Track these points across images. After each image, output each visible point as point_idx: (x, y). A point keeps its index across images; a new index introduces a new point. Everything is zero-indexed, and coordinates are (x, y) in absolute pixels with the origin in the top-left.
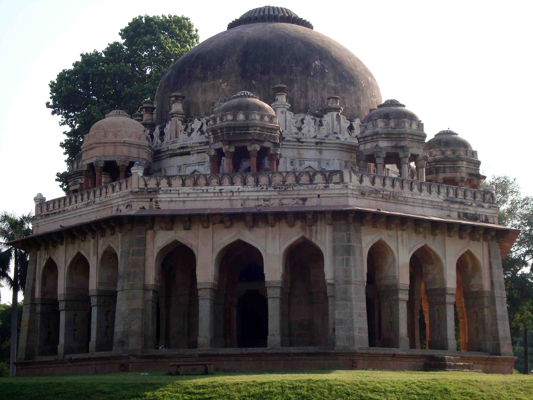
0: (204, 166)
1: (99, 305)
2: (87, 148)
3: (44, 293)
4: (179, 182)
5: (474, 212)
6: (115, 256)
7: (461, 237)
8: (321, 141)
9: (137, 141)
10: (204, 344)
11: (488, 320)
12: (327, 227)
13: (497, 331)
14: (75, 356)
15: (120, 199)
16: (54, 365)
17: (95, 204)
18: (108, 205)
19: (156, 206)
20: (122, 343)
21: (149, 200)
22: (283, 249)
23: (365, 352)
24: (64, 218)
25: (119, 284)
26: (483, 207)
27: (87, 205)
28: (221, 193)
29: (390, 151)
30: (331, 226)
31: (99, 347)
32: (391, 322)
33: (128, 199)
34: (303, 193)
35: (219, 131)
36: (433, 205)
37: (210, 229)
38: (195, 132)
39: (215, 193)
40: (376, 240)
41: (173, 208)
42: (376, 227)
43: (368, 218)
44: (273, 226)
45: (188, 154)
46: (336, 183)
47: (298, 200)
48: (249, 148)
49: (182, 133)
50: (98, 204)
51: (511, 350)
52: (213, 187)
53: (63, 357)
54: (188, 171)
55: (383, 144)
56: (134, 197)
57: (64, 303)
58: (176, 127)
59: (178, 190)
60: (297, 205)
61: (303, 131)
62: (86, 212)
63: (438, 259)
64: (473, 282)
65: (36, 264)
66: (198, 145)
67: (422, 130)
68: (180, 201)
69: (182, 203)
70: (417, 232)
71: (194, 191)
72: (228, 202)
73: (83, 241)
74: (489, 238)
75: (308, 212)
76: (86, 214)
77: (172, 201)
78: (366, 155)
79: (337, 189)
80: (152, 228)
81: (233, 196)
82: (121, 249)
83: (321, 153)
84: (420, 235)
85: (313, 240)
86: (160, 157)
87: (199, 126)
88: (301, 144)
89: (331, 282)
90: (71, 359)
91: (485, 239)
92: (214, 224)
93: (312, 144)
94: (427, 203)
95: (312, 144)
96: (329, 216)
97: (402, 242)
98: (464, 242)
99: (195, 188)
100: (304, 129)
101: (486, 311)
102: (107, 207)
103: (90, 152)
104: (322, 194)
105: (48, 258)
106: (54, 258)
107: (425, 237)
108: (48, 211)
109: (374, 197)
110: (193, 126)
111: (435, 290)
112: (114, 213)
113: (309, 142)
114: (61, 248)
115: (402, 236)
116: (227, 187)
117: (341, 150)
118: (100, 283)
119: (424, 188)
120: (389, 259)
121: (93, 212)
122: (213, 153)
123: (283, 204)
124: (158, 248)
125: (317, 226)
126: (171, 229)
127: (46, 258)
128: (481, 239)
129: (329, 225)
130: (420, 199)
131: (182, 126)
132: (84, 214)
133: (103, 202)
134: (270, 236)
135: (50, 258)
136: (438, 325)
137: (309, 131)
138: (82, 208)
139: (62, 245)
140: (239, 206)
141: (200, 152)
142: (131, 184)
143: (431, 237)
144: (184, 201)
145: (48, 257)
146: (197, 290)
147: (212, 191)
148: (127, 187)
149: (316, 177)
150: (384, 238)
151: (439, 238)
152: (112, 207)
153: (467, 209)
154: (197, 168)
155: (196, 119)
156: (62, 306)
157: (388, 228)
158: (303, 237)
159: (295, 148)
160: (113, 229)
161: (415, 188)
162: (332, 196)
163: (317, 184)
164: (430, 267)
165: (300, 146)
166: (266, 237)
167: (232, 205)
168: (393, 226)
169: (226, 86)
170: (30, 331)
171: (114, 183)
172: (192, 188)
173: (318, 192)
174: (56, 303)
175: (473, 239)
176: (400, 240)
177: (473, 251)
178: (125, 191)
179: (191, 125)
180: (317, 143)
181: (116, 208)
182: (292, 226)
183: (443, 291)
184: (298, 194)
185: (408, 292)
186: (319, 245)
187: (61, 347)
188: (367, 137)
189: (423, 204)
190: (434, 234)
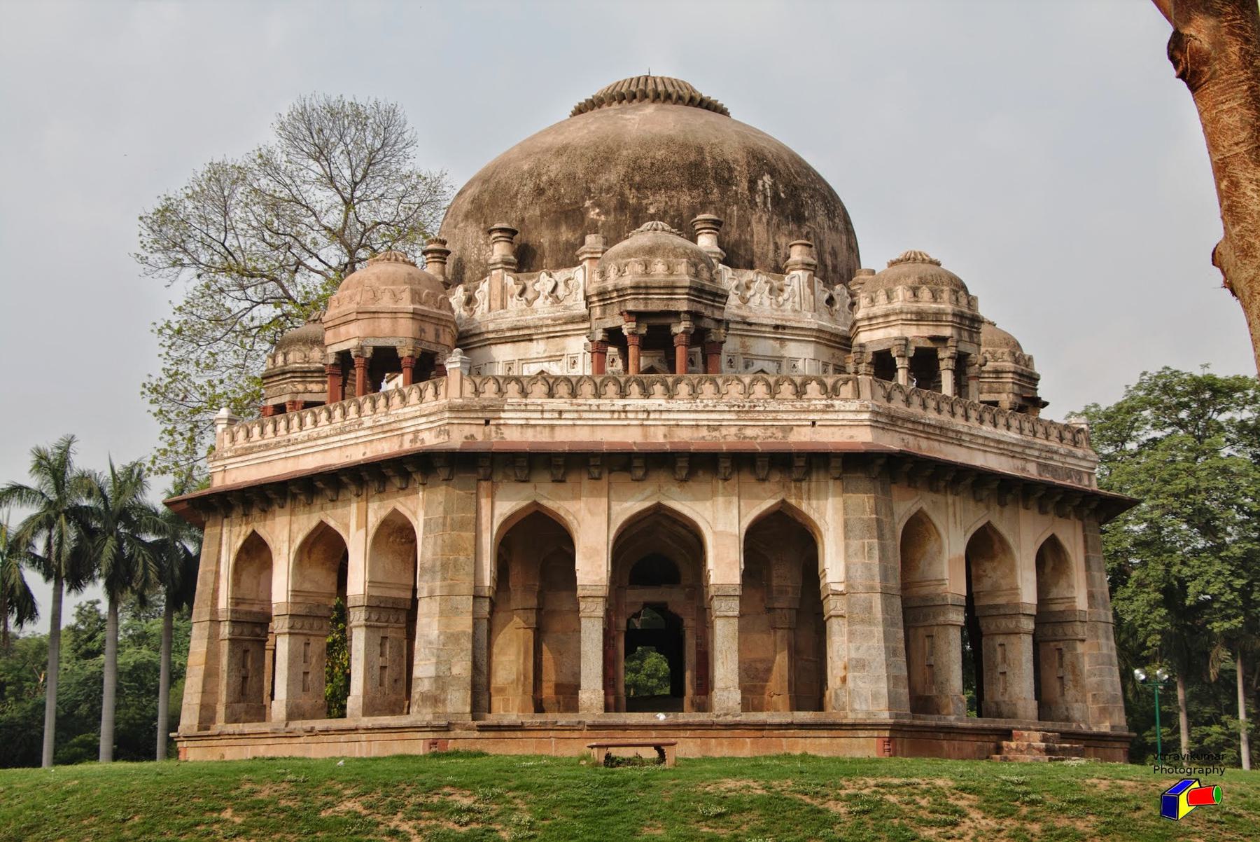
0: (560, 364)
2: (337, 322)
3: (236, 601)
4: (540, 388)
5: (1060, 465)
6: (412, 530)
7: (1043, 511)
8: (784, 323)
9: (435, 310)
10: (592, 704)
12: (831, 483)
14: (308, 724)
15: (424, 420)
16: (270, 741)
17: (364, 429)
18: (391, 431)
19: (497, 433)
21: (483, 422)
22: (745, 523)
23: (907, 721)
24: (288, 455)
26: (1075, 457)
27: (342, 432)
28: (625, 412)
29: (921, 345)
30: (838, 482)
31: (370, 708)
32: (931, 666)
33: (439, 420)
34: (785, 416)
35: (615, 294)
36: (1002, 448)
37: (604, 483)
38: (541, 297)
39: (613, 412)
40: (914, 510)
41: (531, 439)
42: (915, 487)
43: (907, 467)
44: (726, 479)
45: (530, 339)
46: (846, 400)
47: (774, 430)
49: (514, 299)
50: (369, 428)
51: (1124, 723)
52: (608, 401)
53: (287, 725)
54: (531, 370)
55: (912, 332)
56: (453, 415)
57: (287, 621)
58: (503, 288)
59: (541, 405)
60: (770, 440)
61: (749, 304)
62: (340, 444)
63: (1005, 548)
65: (220, 545)
66: (550, 322)
67: (975, 309)
68: (544, 426)
69: (547, 429)
71: (571, 408)
72: (638, 431)
73: (332, 501)
74: (1087, 512)
76: (341, 447)
77: (527, 425)
78: (875, 353)
79: (851, 411)
80: (488, 478)
81: (647, 419)
82: (426, 514)
83: (782, 346)
84: (979, 504)
86: (468, 344)
87: (550, 288)
88: (749, 328)
89: (841, 588)
90: (313, 728)
93: (768, 329)
94: (992, 444)
95: (768, 329)
96: (836, 463)
97: (955, 516)
98: (1046, 519)
99: (575, 401)
100: (752, 300)
102: (389, 434)
103: (343, 329)
104: (820, 420)
105: (248, 533)
106: (262, 532)
107: (988, 508)
108: (249, 442)
109: (910, 429)
110: (537, 287)
112: (407, 446)
113: (762, 325)
115: (954, 504)
116: (635, 401)
117: (818, 343)
118: (372, 583)
119: (973, 414)
120: (931, 547)
121: (357, 444)
122: (599, 336)
123: (745, 438)
124: (501, 515)
125: (810, 481)
127: (243, 532)
128: (1072, 517)
129: (836, 479)
130: (981, 437)
131: (515, 286)
132: (334, 448)
133: (382, 425)
135: (254, 532)
136: (1004, 673)
137: (761, 304)
138: (332, 436)
139: (282, 507)
140: (661, 440)
141: (553, 337)
142: (446, 389)
143: (998, 508)
144: (552, 426)
145: (250, 531)
147: (609, 408)
148: (436, 394)
149: (809, 387)
150: (925, 508)
151: (1008, 511)
152: (402, 435)
153: (1051, 459)
154: (545, 366)
155: (544, 274)
159: (738, 335)
162: (840, 423)
163: (809, 400)
165: (747, 331)
167: (645, 436)
168: (942, 484)
169: (598, 214)
170: (210, 674)
172: (568, 401)
173: (813, 416)
175: (1062, 515)
176: (951, 510)
178: (434, 403)
179: (533, 285)
180: (777, 327)
181: (411, 436)
182: (763, 480)
184: (775, 420)
185: (963, 609)
186: (814, 516)
187: (278, 708)
188: (876, 317)
189: (984, 445)
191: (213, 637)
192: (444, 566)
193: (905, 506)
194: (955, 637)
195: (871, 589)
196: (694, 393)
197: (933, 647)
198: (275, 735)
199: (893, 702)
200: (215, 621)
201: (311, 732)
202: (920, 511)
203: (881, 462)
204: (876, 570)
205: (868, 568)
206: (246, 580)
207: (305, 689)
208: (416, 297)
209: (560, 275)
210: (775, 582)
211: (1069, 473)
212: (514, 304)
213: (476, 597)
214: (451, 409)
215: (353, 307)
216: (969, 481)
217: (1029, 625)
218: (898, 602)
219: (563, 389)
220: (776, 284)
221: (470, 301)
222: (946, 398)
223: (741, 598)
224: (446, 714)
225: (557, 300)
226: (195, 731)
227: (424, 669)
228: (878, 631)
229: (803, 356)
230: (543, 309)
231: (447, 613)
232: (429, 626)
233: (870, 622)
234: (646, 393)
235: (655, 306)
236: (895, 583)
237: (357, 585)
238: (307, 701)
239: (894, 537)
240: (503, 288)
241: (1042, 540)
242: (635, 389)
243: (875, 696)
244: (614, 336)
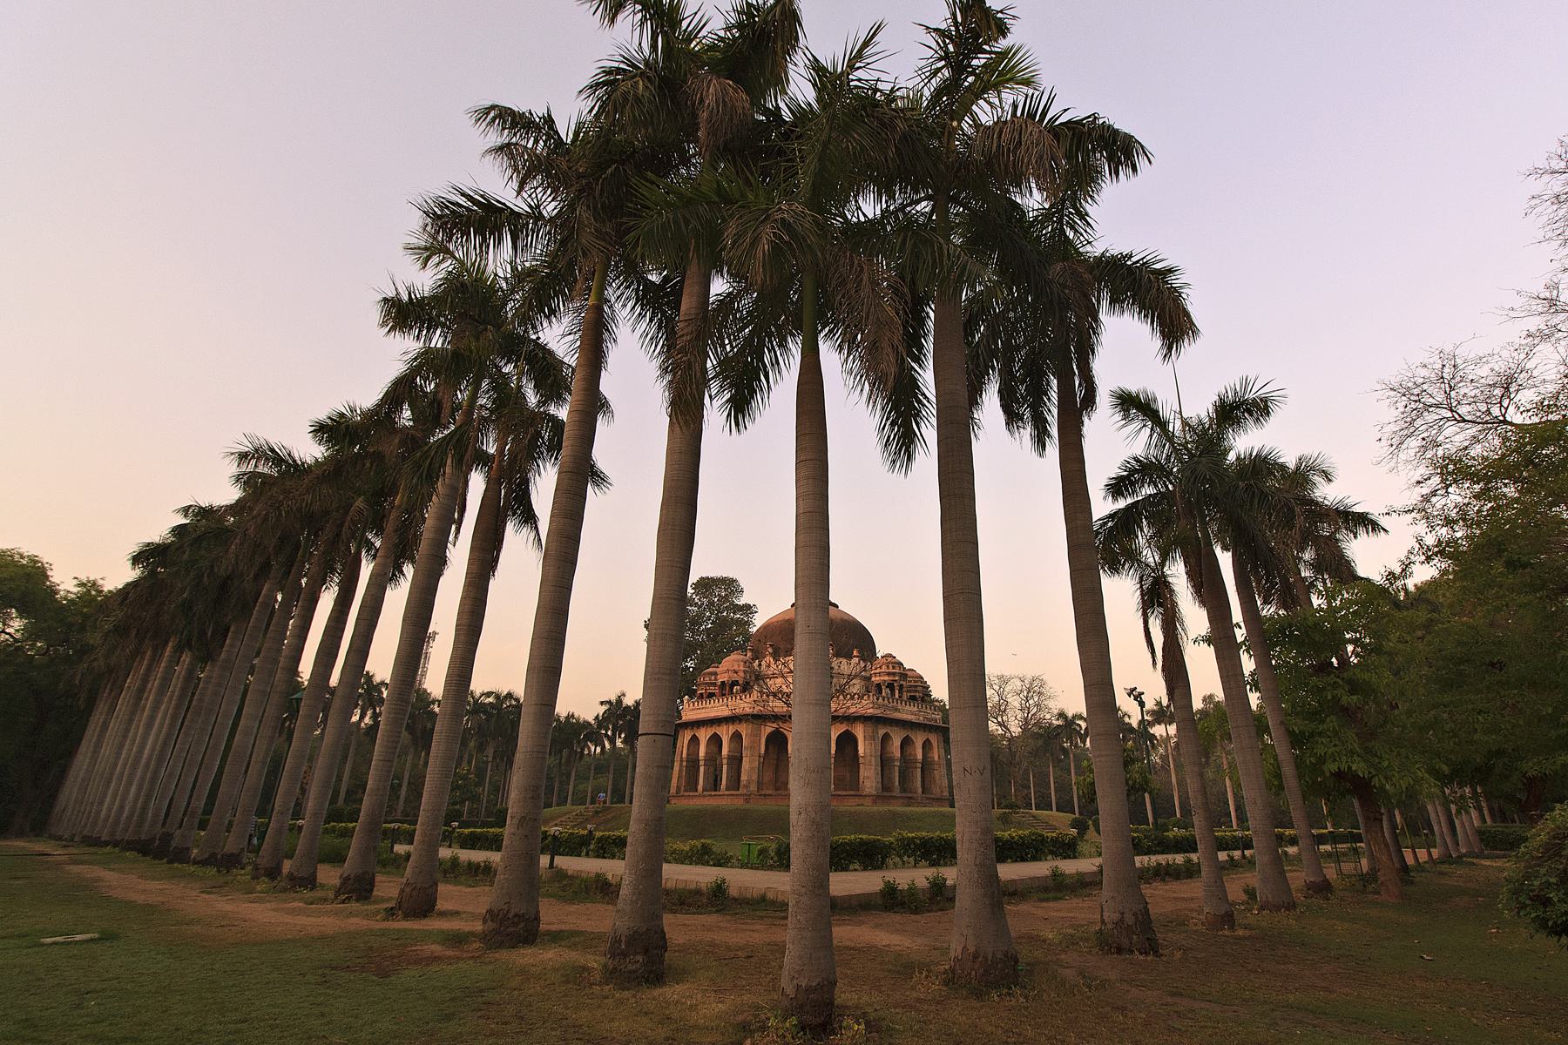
3: (688, 754)
7: (925, 731)
11: (937, 777)
20: (746, 787)
55: (886, 678)
64: (929, 755)
118: (729, 751)
120: (891, 742)
156: (702, 763)
161: (903, 703)
175: (930, 732)
177: (930, 739)
187: (700, 787)
191: (681, 765)
194: (897, 769)
198: (699, 796)
200: (681, 761)
227: (744, 778)
232: (746, 765)
237: (725, 751)
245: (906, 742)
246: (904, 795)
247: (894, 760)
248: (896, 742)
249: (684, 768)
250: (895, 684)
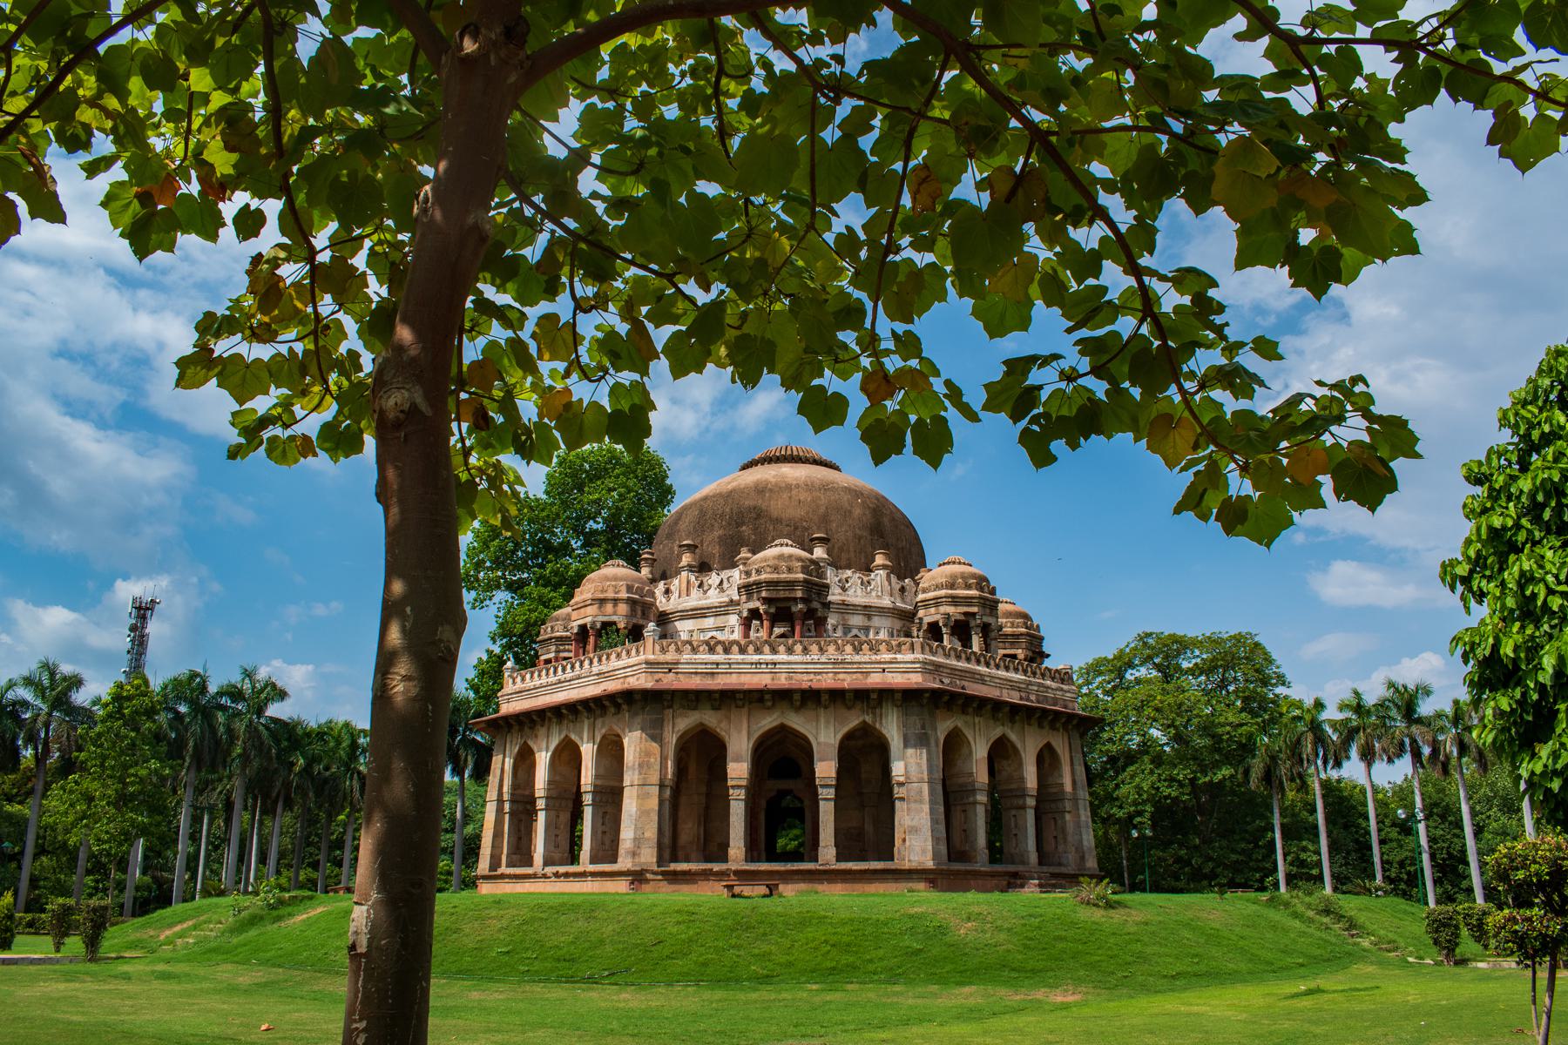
1: (594, 804)
7: (1041, 726)
11: (1070, 827)
13: (1081, 841)
22: (839, 736)
25: (626, 777)
40: (952, 727)
44: (826, 707)
45: (704, 616)
48: (794, 609)
51: (1096, 866)
55: (951, 610)
70: (995, 718)
75: (873, 690)
80: (670, 707)
83: (869, 617)
85: (878, 726)
87: (718, 582)
89: (902, 779)
91: (1066, 729)
92: (750, 703)
96: (898, 696)
101: (1068, 817)
106: (531, 743)
111: (1011, 790)
114: (542, 731)
118: (597, 776)
120: (965, 751)
122: (745, 614)
126: (695, 708)
134: (822, 720)
146: (727, 788)
154: (714, 633)
156: (541, 804)
157: (964, 712)
158: (864, 722)
160: (618, 707)
164: (1005, 763)
166: (818, 721)
170: (498, 834)
171: (619, 649)
174: (532, 800)
175: (1053, 728)
177: (1054, 744)
182: (849, 708)
183: (1023, 793)
186: (884, 732)
190: (1012, 721)
191: (500, 810)
192: (641, 766)
193: (943, 727)
195: (921, 781)
196: (806, 650)
197: (966, 817)
198: (534, 876)
199: (935, 856)
200: (500, 801)
201: (557, 875)
202: (956, 728)
203: (927, 695)
204: (925, 767)
205: (919, 764)
206: (520, 773)
207: (557, 846)
208: (629, 589)
209: (725, 574)
210: (863, 776)
211: (1055, 701)
212: (695, 592)
213: (662, 786)
214: (647, 663)
215: (589, 596)
216: (989, 707)
217: (1031, 802)
218: (939, 788)
219: (719, 648)
220: (865, 579)
221: (667, 591)
222: (975, 653)
223: (838, 787)
224: (640, 864)
225: (722, 591)
226: (486, 872)
227: (627, 834)
228: (926, 808)
229: (882, 630)
230: (714, 598)
231: (642, 797)
233: (921, 802)
234: (790, 651)
235: (782, 595)
236: (939, 775)
238: (557, 856)
239: (937, 745)
240: (688, 582)
241: (1041, 745)
242: (767, 649)
243: (924, 851)
244: (754, 614)
245: (1001, 752)
246: (998, 868)
247: (974, 791)
248: (980, 751)
249: (507, 816)
250: (972, 623)
